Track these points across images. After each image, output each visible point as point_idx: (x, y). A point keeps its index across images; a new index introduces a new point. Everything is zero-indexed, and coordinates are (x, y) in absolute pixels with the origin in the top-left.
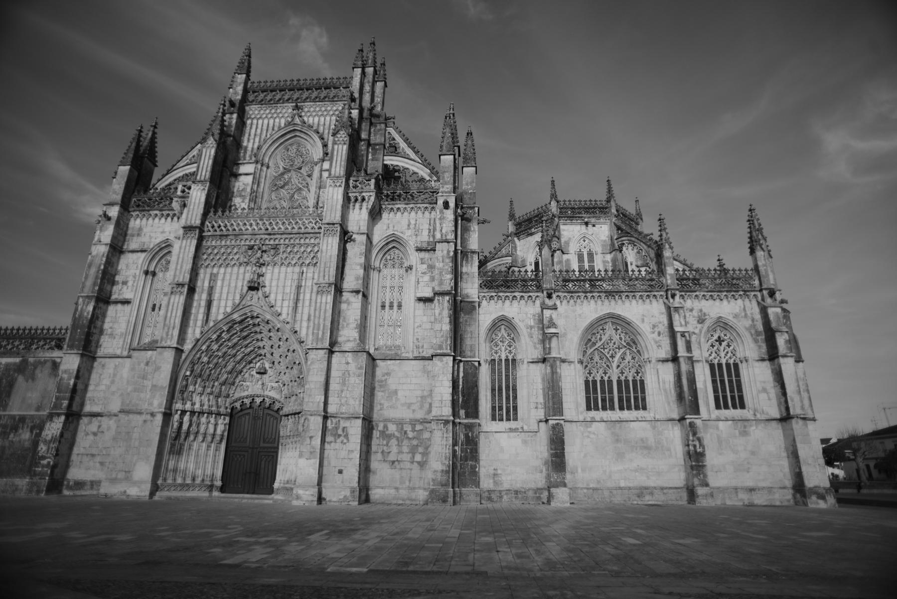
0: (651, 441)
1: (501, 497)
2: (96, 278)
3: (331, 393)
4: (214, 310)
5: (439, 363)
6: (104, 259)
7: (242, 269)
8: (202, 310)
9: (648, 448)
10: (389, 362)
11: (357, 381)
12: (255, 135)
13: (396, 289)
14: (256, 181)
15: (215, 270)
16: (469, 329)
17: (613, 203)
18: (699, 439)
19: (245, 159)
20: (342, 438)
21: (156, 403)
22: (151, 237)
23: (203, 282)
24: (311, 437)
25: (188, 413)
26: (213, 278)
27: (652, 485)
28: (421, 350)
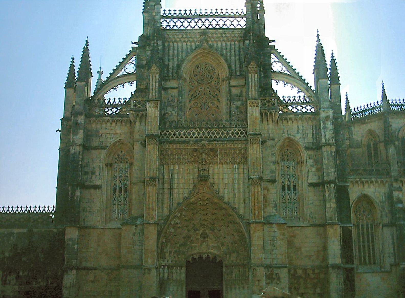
4: (175, 195)
5: (331, 229)
7: (191, 167)
8: (166, 196)
10: (294, 229)
12: (173, 55)
14: (180, 93)
15: (172, 167)
19: (168, 76)
20: (275, 280)
21: (150, 261)
24: (259, 281)
25: (166, 267)
26: (172, 172)
28: (314, 220)
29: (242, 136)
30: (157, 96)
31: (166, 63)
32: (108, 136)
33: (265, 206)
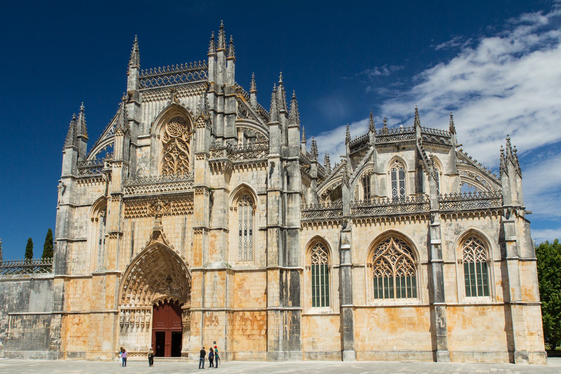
0: (416, 319)
1: (317, 356)
2: (65, 227)
3: (206, 296)
4: (135, 246)
6: (67, 214)
8: (129, 246)
9: (413, 324)
11: (222, 288)
12: (149, 114)
13: (248, 222)
16: (293, 247)
17: (418, 129)
18: (443, 319)
20: (215, 323)
21: (109, 306)
22: (92, 195)
23: (127, 229)
24: (196, 323)
27: (415, 349)
28: (263, 263)
29: (191, 187)
30: (121, 157)
31: (142, 122)
32: (93, 193)
33: (213, 253)
